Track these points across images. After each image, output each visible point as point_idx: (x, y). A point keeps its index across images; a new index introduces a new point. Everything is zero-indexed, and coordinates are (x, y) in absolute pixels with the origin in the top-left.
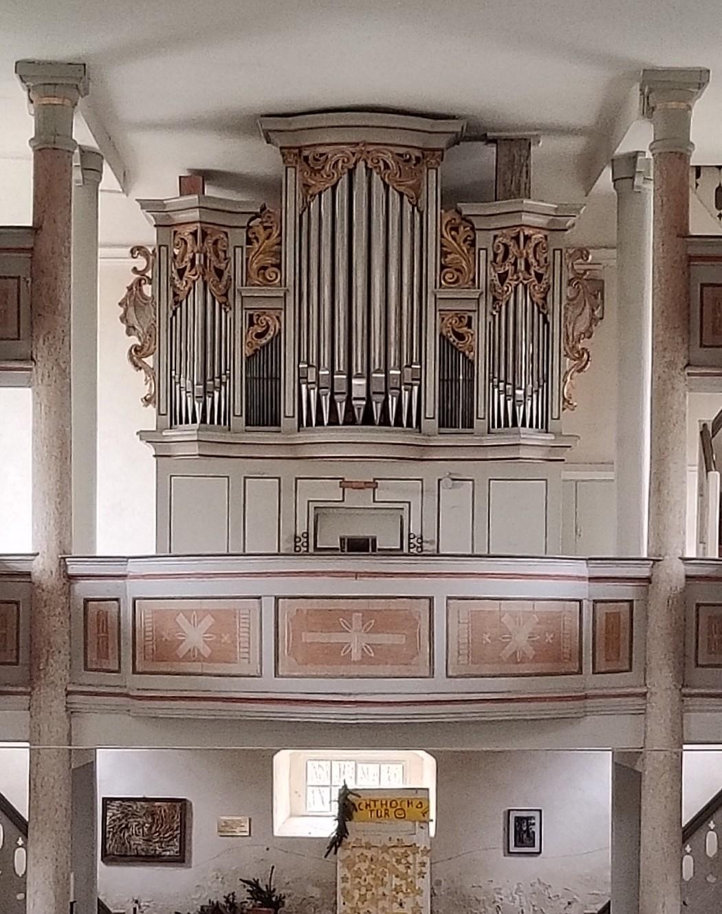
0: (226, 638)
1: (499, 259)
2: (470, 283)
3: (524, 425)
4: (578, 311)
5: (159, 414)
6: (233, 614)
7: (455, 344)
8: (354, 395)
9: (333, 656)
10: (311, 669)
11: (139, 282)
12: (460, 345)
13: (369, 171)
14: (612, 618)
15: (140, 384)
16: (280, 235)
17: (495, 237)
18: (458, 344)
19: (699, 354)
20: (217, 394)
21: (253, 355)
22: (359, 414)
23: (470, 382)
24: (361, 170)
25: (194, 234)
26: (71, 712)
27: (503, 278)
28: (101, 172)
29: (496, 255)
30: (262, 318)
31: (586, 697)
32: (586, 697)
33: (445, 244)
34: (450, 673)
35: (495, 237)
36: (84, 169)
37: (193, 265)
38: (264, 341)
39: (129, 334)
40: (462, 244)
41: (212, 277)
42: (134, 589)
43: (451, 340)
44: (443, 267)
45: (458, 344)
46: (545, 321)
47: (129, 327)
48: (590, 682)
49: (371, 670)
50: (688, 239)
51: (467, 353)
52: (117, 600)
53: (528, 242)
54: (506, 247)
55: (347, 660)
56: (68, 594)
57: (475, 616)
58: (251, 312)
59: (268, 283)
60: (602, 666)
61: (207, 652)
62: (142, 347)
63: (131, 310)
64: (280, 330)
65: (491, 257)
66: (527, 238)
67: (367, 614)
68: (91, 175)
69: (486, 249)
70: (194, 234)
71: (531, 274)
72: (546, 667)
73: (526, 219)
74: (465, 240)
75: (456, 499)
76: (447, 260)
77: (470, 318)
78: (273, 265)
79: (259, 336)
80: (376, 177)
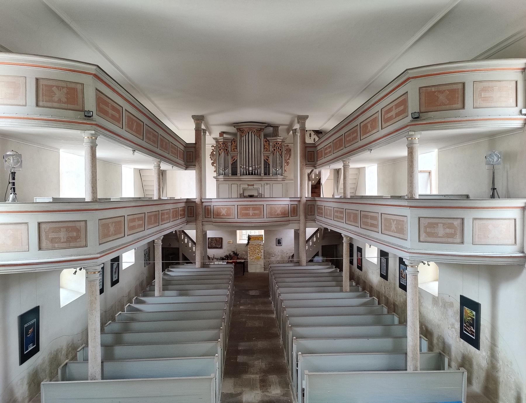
0: (229, 212)
1: (274, 147)
3: (278, 175)
5: (217, 174)
6: (230, 208)
8: (250, 170)
9: (247, 215)
10: (243, 217)
13: (252, 132)
14: (294, 208)
15: (213, 169)
17: (273, 143)
19: (308, 163)
22: (251, 173)
23: (269, 167)
24: (250, 132)
25: (222, 143)
27: (274, 150)
28: (206, 133)
29: (273, 146)
31: (290, 221)
32: (290, 221)
35: (273, 143)
36: (203, 133)
37: (222, 149)
39: (211, 160)
42: (213, 204)
44: (264, 148)
46: (282, 157)
48: (290, 218)
49: (254, 217)
54: (275, 145)
55: (250, 215)
56: (202, 205)
59: (234, 151)
61: (226, 214)
63: (212, 156)
65: (272, 147)
66: (278, 143)
67: (253, 208)
68: (205, 133)
70: (222, 143)
72: (283, 216)
73: (278, 140)
75: (267, 187)
78: (236, 148)
79: (234, 160)
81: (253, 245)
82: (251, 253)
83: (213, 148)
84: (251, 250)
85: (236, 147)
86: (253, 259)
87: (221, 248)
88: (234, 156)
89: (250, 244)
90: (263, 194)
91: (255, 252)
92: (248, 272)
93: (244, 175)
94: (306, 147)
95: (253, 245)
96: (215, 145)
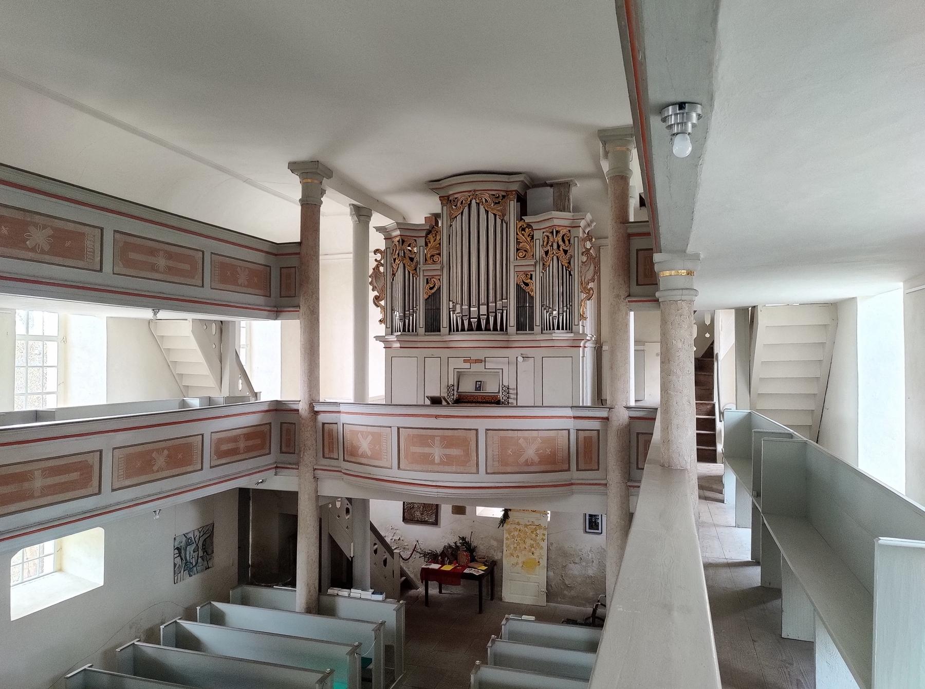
1: (545, 243)
3: (558, 328)
4: (587, 268)
5: (386, 327)
9: (425, 461)
11: (378, 265)
12: (527, 289)
13: (478, 204)
14: (588, 440)
16: (440, 239)
17: (543, 233)
19: (635, 289)
20: (411, 318)
21: (428, 298)
22: (474, 326)
23: (532, 307)
26: (316, 478)
27: (547, 253)
29: (543, 242)
30: (432, 280)
31: (572, 484)
32: (572, 484)
34: (488, 471)
35: (543, 233)
38: (433, 291)
41: (407, 261)
42: (344, 418)
43: (522, 286)
44: (518, 250)
46: (570, 274)
47: (373, 287)
49: (447, 468)
50: (628, 224)
51: (530, 293)
52: (336, 424)
53: (559, 234)
54: (548, 237)
55: (432, 462)
57: (503, 439)
58: (426, 277)
59: (434, 262)
60: (581, 466)
61: (369, 453)
62: (379, 297)
64: (440, 286)
65: (541, 244)
67: (443, 438)
68: (362, 218)
70: (399, 241)
72: (548, 468)
73: (556, 222)
75: (525, 367)
77: (531, 275)
78: (437, 254)
79: (431, 288)
80: (481, 207)
81: (518, 524)
82: (512, 546)
83: (379, 256)
84: (513, 537)
86: (517, 563)
87: (437, 525)
88: (433, 277)
89: (511, 519)
90: (513, 389)
91: (524, 546)
92: (501, 599)
93: (457, 330)
94: (630, 236)
95: (518, 524)
96: (383, 248)
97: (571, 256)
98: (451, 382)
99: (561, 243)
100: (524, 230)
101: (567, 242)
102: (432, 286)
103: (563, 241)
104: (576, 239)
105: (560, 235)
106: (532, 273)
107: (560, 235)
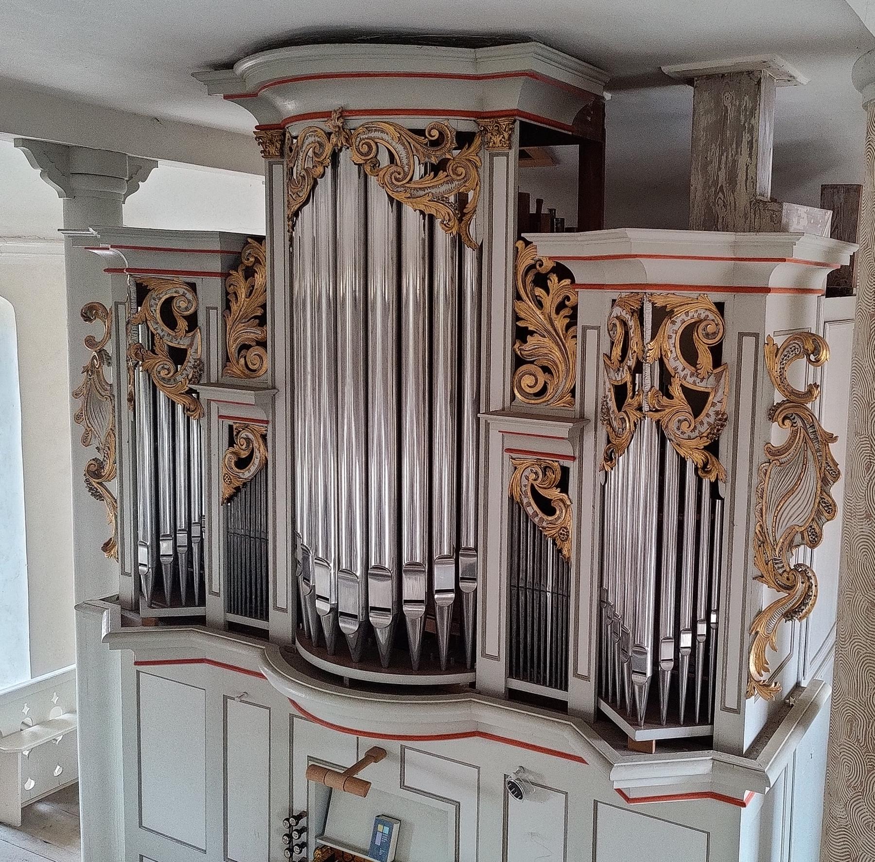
1: (617, 351)
2: (568, 398)
4: (788, 482)
7: (536, 520)
18: (542, 520)
27: (620, 392)
30: (243, 434)
33: (522, 315)
40: (554, 315)
41: (162, 364)
43: (530, 511)
44: (519, 361)
45: (542, 520)
46: (715, 494)
51: (558, 542)
58: (231, 422)
65: (605, 348)
69: (598, 328)
71: (670, 397)
74: (560, 307)
76: (526, 347)
77: (565, 471)
79: (243, 463)
85: (254, 333)
97: (722, 420)
98: (299, 806)
99: (676, 362)
100: (541, 281)
101: (705, 359)
102: (244, 455)
103: (689, 354)
104: (749, 343)
105: (673, 329)
106: (566, 463)
107: (673, 329)
